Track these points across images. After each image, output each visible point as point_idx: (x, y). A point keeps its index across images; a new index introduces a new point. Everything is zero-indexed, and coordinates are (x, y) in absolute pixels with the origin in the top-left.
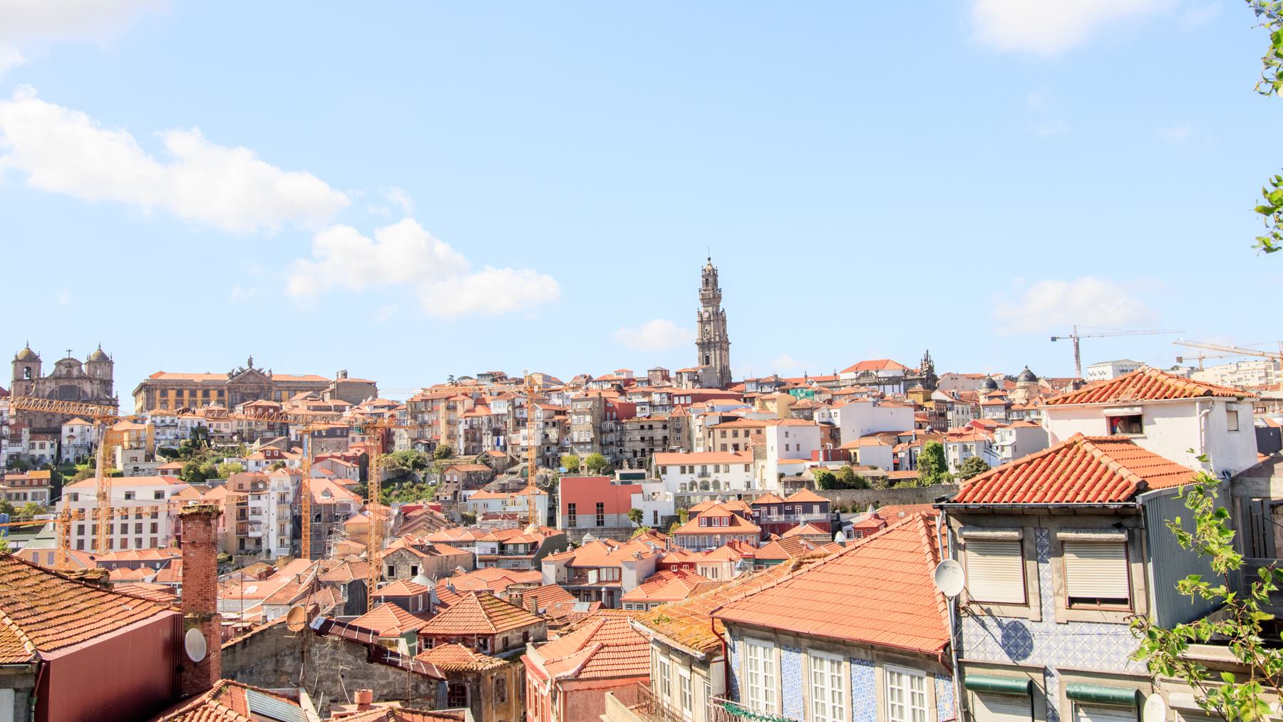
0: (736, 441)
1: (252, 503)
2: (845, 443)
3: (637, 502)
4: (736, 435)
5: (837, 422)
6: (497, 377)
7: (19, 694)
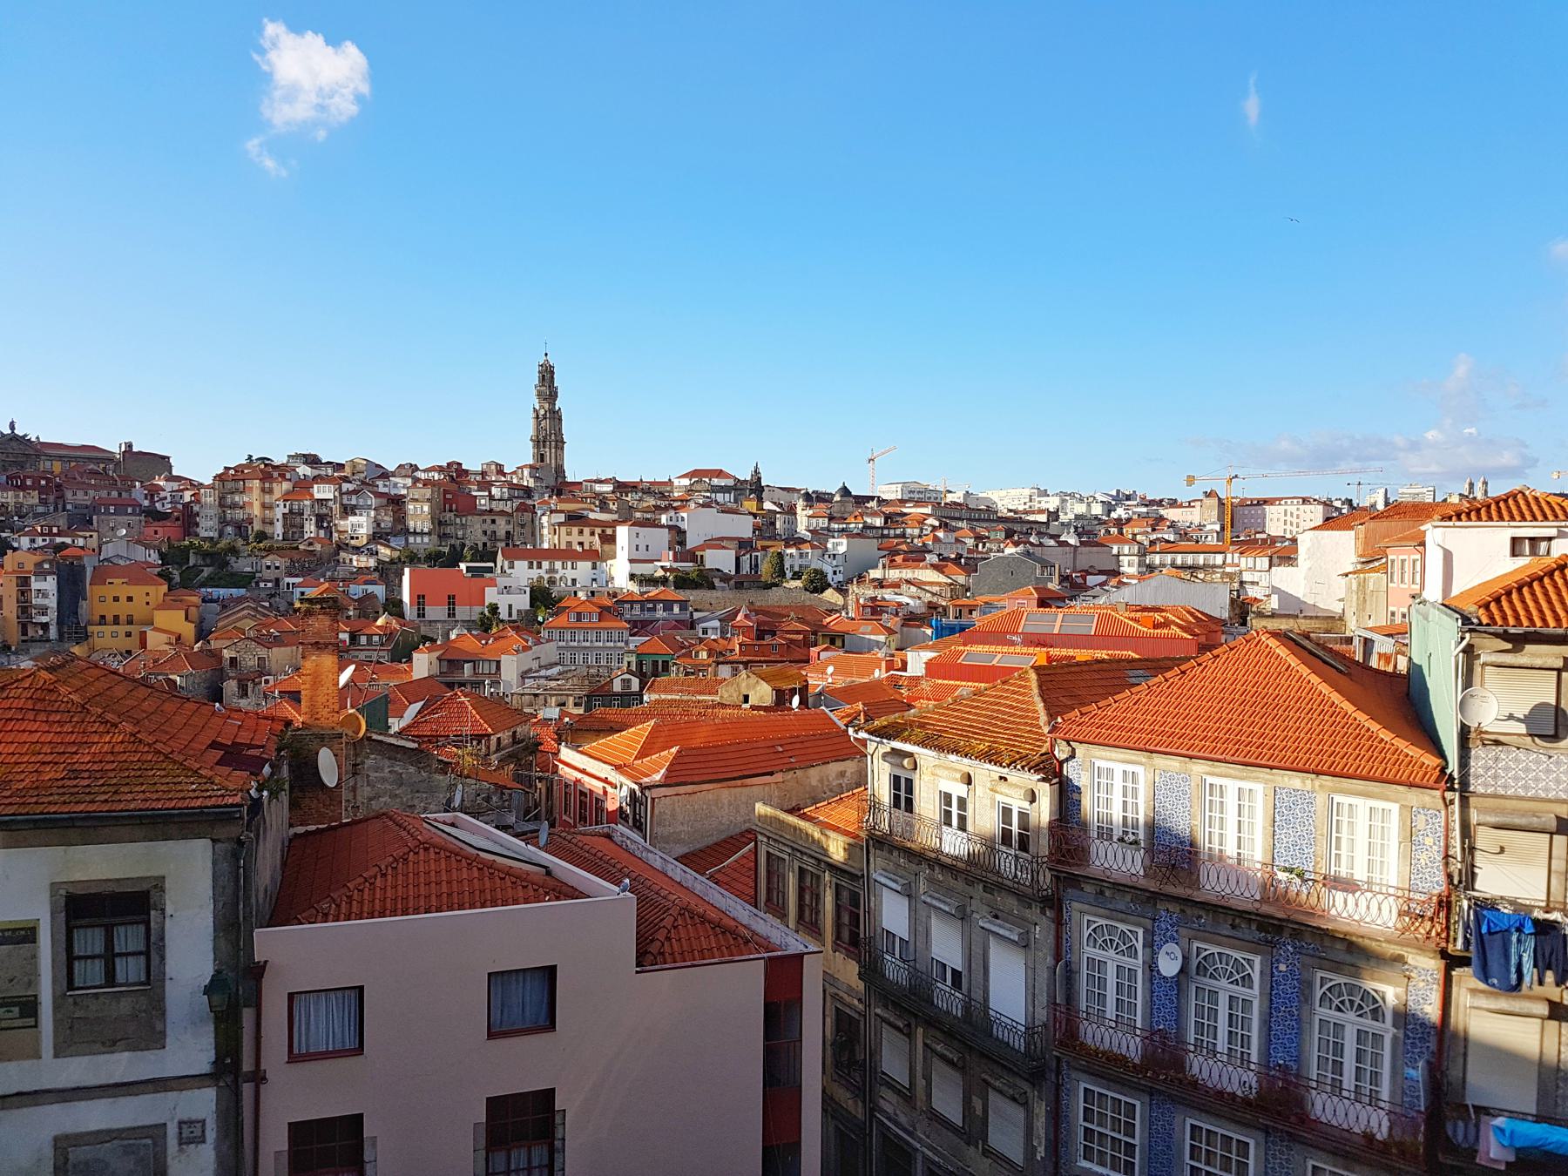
0: (581, 539)
1: (35, 585)
2: (691, 544)
3: (491, 595)
4: (581, 532)
5: (684, 526)
6: (312, 460)
7: (218, 846)
